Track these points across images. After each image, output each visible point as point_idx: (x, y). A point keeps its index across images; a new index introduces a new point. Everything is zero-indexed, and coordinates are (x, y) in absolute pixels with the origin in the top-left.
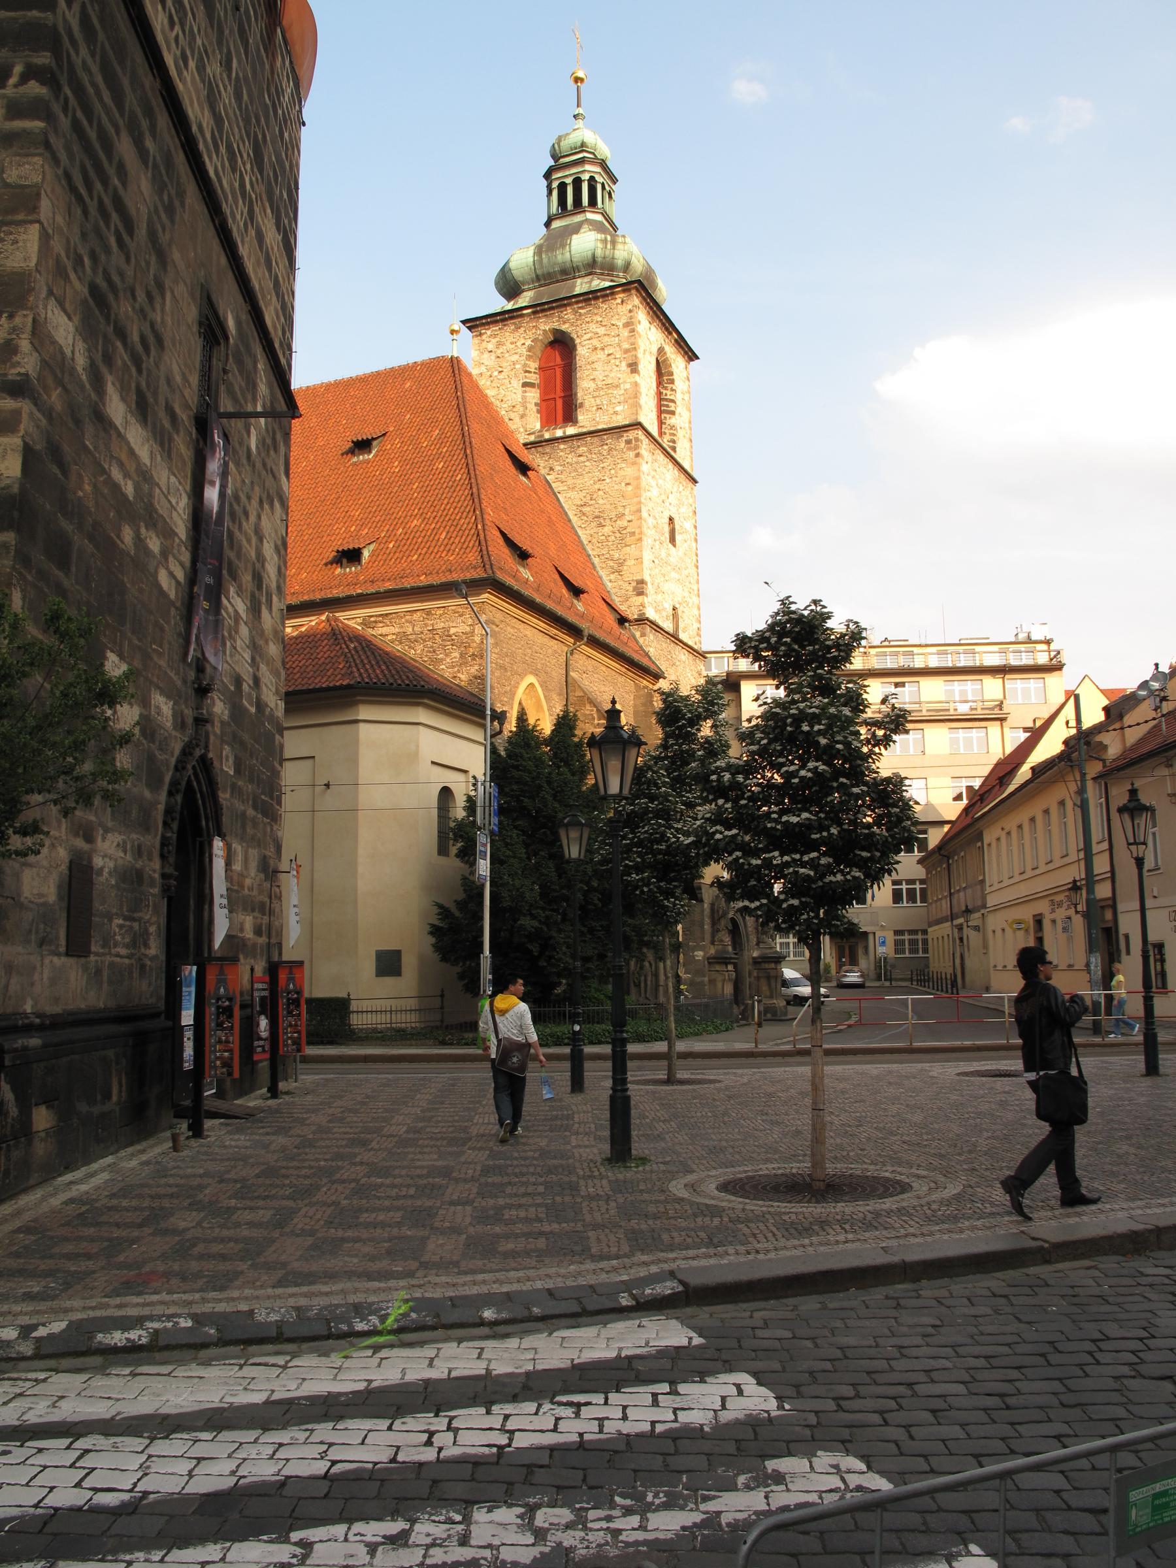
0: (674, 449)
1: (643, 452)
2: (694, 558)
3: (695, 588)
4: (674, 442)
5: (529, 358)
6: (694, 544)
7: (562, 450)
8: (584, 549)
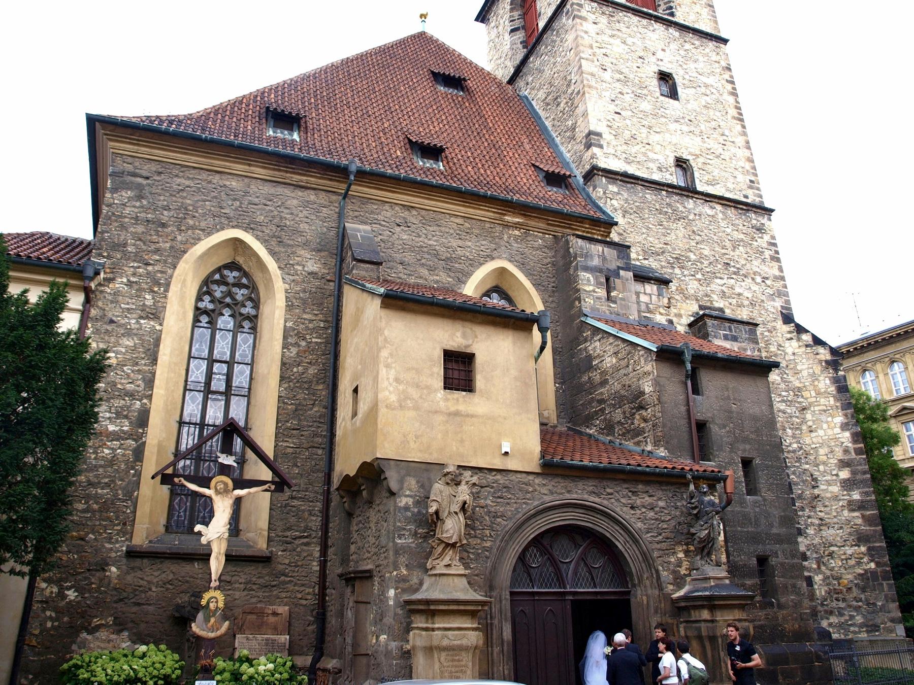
0: (672, 14)
1: (583, 13)
2: (733, 112)
3: (740, 141)
4: (671, 8)
5: (512, 10)
6: (731, 99)
7: (533, 62)
8: (551, 136)
